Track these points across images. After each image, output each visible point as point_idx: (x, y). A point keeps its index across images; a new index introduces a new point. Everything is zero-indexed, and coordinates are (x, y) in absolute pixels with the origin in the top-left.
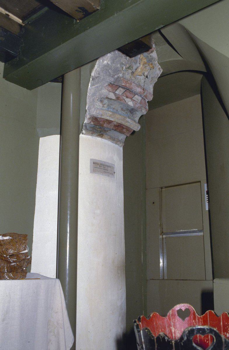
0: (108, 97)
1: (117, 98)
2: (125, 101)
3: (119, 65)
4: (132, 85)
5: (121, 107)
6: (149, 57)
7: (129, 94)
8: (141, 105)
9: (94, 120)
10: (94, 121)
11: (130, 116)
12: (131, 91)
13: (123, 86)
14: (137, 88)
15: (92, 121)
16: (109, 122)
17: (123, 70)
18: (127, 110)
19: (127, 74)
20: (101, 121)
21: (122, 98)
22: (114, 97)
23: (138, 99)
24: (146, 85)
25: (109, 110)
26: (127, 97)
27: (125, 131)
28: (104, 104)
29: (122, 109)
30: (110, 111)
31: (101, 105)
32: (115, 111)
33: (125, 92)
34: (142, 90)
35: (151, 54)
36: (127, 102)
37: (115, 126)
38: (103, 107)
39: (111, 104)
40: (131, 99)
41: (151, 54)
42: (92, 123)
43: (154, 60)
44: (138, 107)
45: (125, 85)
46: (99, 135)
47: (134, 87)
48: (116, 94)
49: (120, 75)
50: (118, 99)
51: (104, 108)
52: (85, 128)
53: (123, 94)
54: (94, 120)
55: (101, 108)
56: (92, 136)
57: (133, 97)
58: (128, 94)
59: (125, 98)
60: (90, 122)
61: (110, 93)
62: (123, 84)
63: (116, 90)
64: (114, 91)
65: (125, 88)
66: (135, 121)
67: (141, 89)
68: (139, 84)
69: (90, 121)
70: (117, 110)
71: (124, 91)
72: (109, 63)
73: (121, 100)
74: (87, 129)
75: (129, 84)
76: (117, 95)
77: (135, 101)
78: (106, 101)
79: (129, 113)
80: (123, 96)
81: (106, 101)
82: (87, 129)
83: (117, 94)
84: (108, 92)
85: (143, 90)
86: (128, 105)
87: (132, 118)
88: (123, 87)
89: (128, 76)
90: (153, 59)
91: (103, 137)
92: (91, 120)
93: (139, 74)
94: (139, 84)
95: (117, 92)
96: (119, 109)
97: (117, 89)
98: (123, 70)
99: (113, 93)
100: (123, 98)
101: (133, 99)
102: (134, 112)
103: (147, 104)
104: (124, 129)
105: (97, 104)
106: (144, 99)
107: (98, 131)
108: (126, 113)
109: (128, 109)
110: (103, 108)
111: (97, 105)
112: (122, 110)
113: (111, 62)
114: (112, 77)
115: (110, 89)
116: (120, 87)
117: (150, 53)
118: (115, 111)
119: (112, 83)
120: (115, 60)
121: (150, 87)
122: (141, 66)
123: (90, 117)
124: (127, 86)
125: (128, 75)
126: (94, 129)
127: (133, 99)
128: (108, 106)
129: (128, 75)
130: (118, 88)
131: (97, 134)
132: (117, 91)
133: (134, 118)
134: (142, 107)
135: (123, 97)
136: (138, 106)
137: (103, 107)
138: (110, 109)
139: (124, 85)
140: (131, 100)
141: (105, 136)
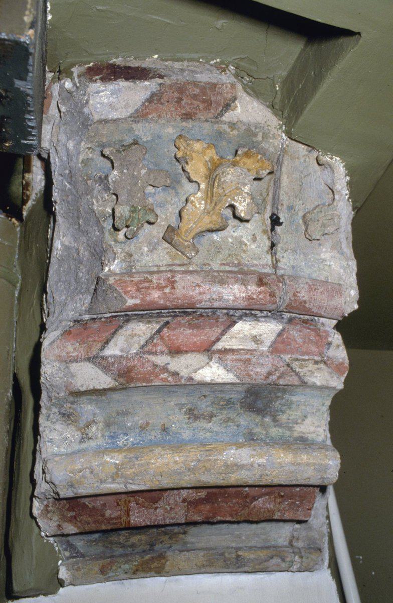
0: (73, 389)
1: (119, 376)
2: (175, 374)
3: (96, 228)
4: (179, 285)
5: (181, 406)
6: (225, 132)
7: (189, 331)
8: (287, 357)
9: (73, 514)
10: (75, 517)
11: (257, 430)
12: (201, 315)
13: (134, 308)
14: (217, 288)
15: (64, 518)
16: (152, 496)
17: (116, 241)
18: (222, 408)
19: (146, 249)
20: (104, 505)
21: (148, 368)
22: (104, 380)
23: (256, 339)
24: (286, 261)
25: (120, 443)
26: (176, 351)
27: (272, 506)
28: (88, 426)
29: (193, 414)
30: (119, 450)
31: (71, 433)
32: (154, 435)
33: (159, 331)
34: (253, 288)
35: (227, 117)
36: (184, 373)
37: (193, 504)
38: (82, 440)
39: (126, 413)
40: (208, 350)
41: (227, 114)
42: (70, 528)
43: (265, 136)
44: (270, 374)
45: (142, 299)
46: (142, 564)
47: (197, 290)
48: (105, 358)
49: (112, 268)
50: (130, 380)
51: (92, 444)
52: (67, 554)
53: (149, 347)
54: (73, 514)
55: (77, 447)
56: (108, 580)
57: (218, 340)
58: (184, 334)
59: (161, 360)
60: (59, 526)
61: (74, 367)
62: (130, 302)
63: (108, 341)
64: (94, 351)
65: (151, 316)
66: (304, 443)
67: (244, 283)
68: (239, 264)
69: (54, 524)
70: (165, 430)
71: (157, 327)
72: (67, 241)
73: (145, 379)
74: (83, 556)
75: (160, 288)
76: (113, 364)
77: (233, 351)
78: (87, 409)
79: (245, 420)
80: (151, 353)
81: (89, 407)
82: (83, 556)
83: (110, 360)
84: (63, 366)
85: (261, 282)
86: (212, 386)
87: (274, 431)
88: (145, 312)
89: (155, 256)
90: (256, 135)
91: (167, 568)
92: (55, 518)
93: (206, 223)
94: (239, 264)
95: (113, 350)
96: (178, 421)
97: (114, 333)
98: (116, 241)
99: (91, 359)
100: (156, 366)
101: (219, 346)
102: (270, 402)
103: (337, 338)
104: (254, 499)
105: (54, 436)
106: (305, 322)
107: (133, 546)
108: (228, 420)
109: (229, 402)
110: (84, 446)
111: (51, 441)
112: (197, 418)
113: (73, 236)
114: (87, 291)
115: (70, 348)
116: (128, 321)
117: (221, 114)
118: (154, 435)
119: (87, 317)
120: (78, 217)
121: (323, 256)
122: (203, 186)
123: (47, 506)
124: (153, 302)
125: (151, 251)
126: (111, 543)
127: (219, 346)
128: (108, 425)
129: (151, 251)
130: (121, 327)
131: (127, 566)
132: (111, 344)
133: (290, 429)
134: (295, 365)
135: (149, 361)
136: (264, 371)
137: (82, 440)
138: (126, 434)
139: (138, 301)
140: (201, 358)
141: (175, 558)
